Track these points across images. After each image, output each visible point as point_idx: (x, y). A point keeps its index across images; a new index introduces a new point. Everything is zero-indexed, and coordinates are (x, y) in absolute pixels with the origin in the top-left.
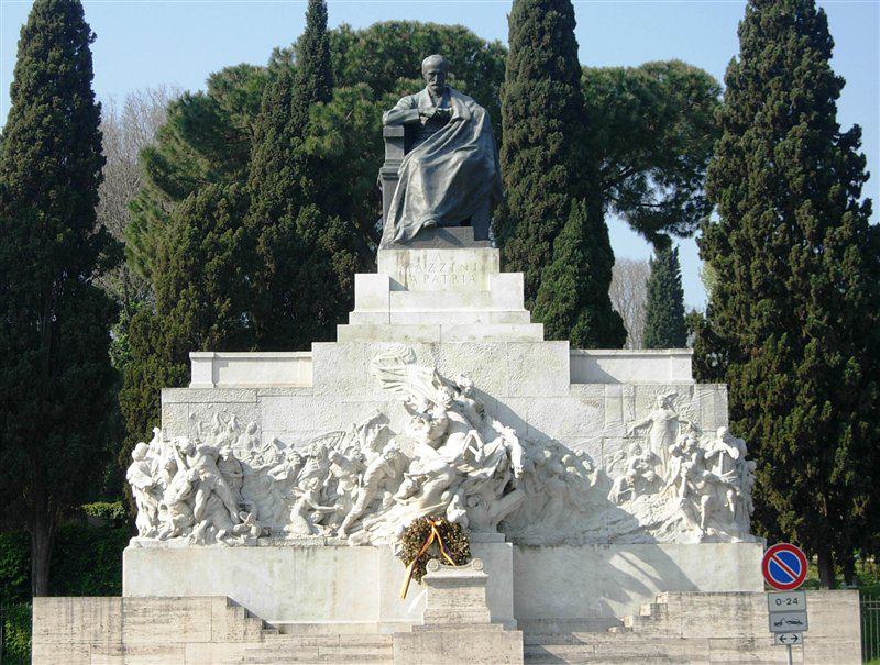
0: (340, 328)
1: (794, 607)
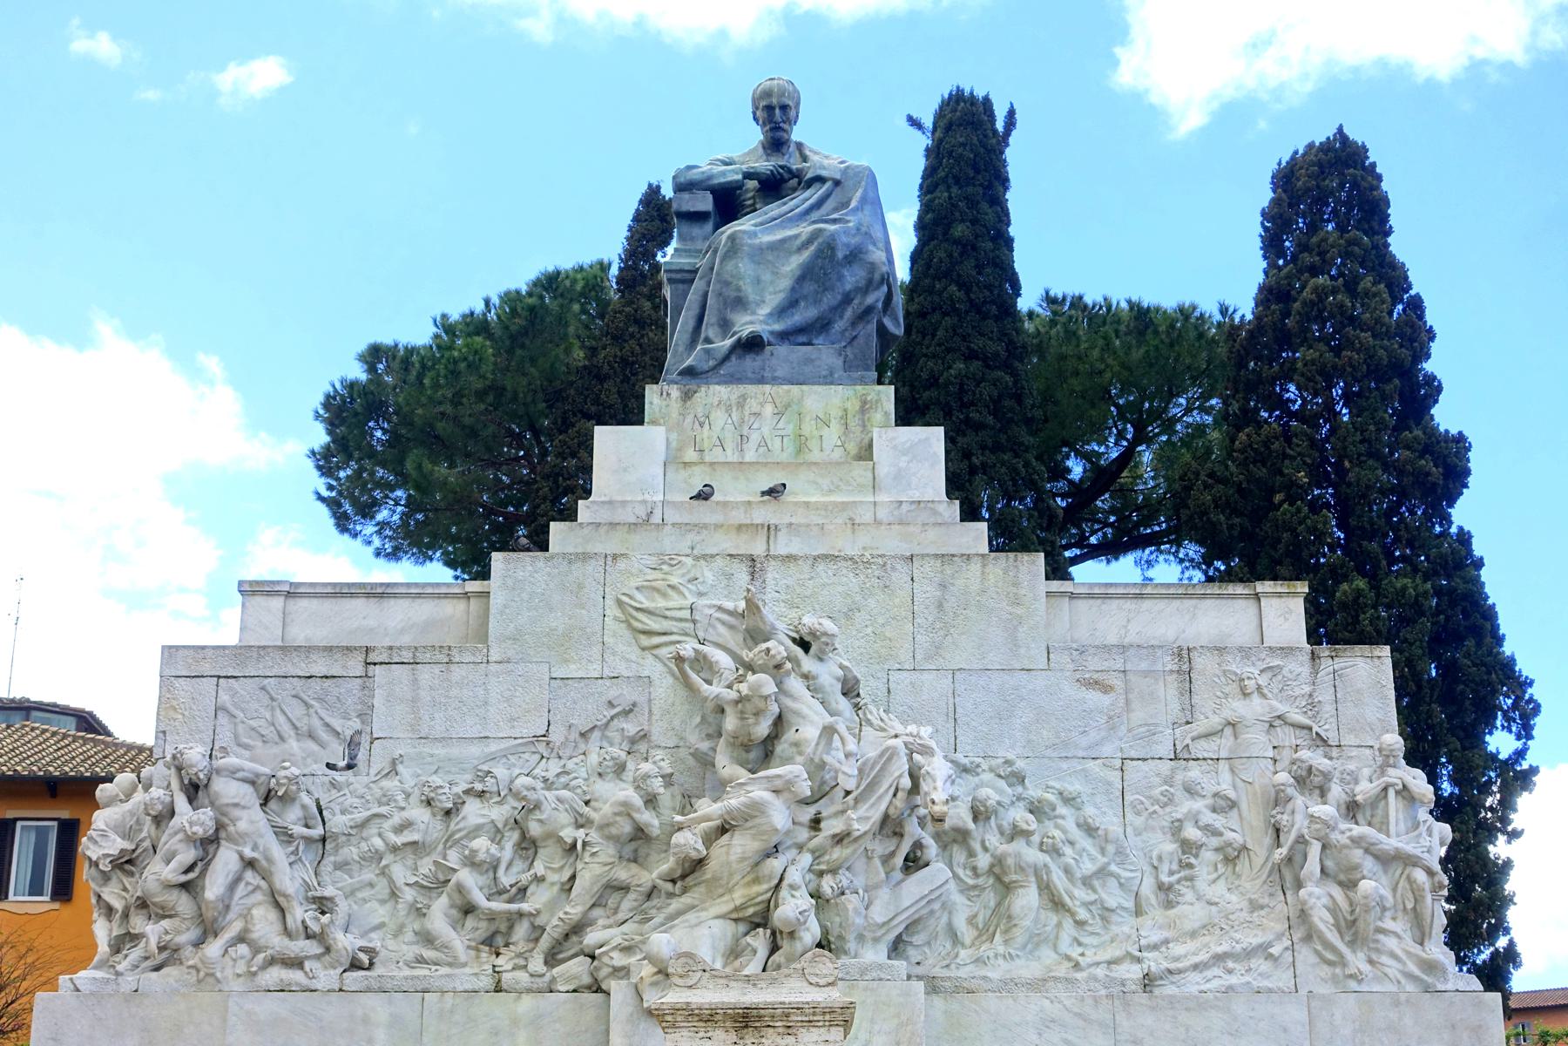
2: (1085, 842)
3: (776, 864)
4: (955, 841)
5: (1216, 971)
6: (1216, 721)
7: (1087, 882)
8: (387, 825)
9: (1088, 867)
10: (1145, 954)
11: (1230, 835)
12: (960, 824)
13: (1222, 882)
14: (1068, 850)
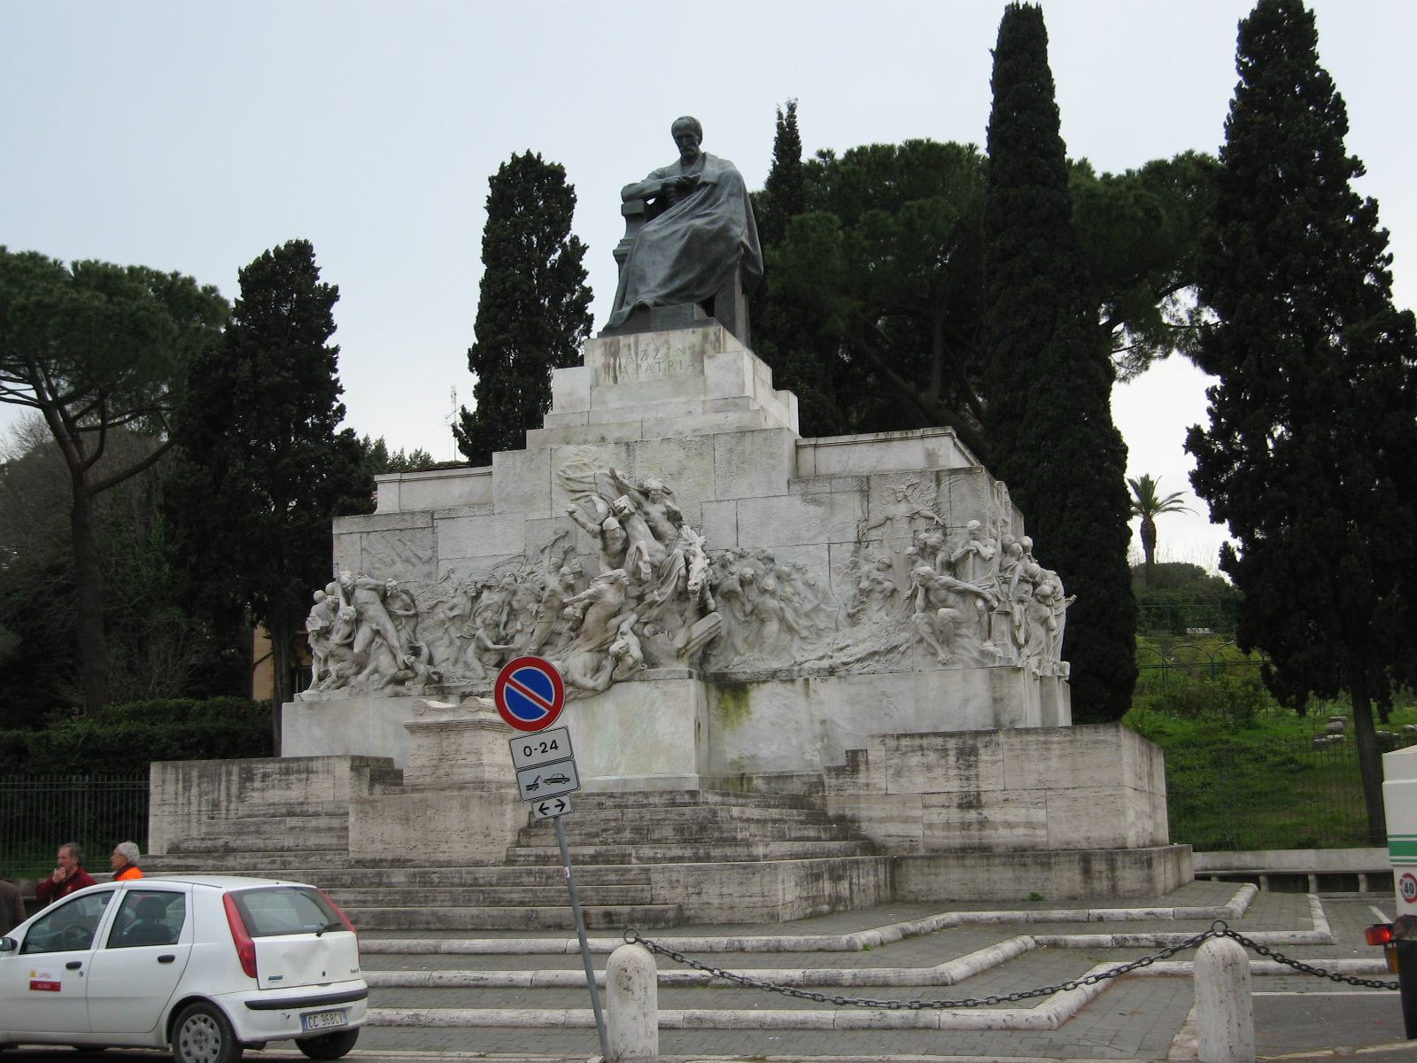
0: (530, 434)
1: (552, 755)
2: (809, 594)
3: (614, 622)
5: (869, 662)
6: (881, 517)
7: (807, 615)
8: (446, 606)
9: (808, 606)
10: (836, 654)
11: (886, 584)
12: (732, 588)
13: (884, 610)
14: (796, 599)
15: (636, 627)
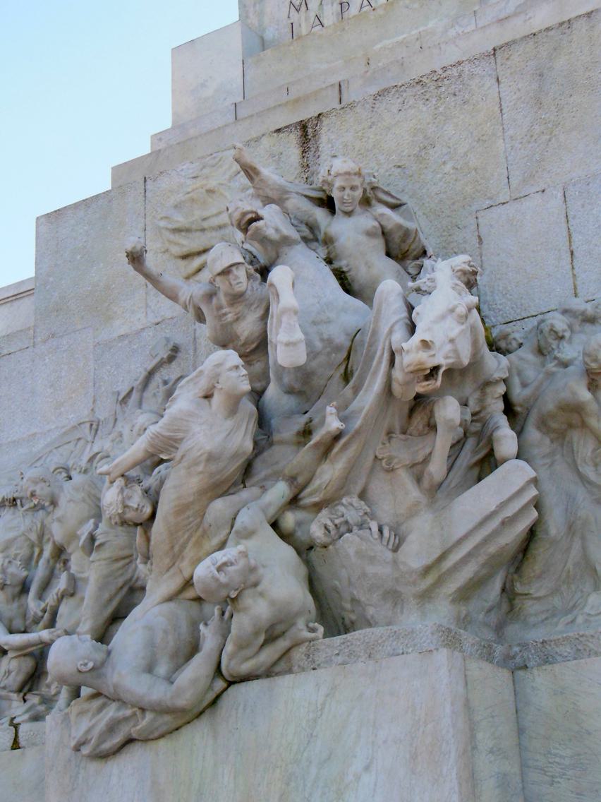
4: (571, 426)
15: (289, 520)
